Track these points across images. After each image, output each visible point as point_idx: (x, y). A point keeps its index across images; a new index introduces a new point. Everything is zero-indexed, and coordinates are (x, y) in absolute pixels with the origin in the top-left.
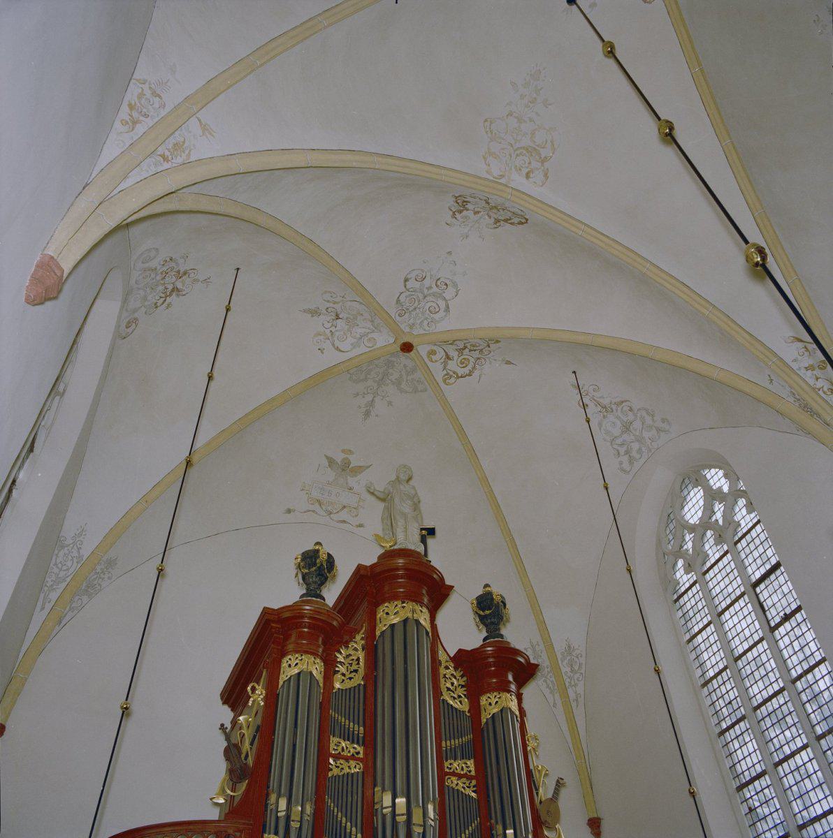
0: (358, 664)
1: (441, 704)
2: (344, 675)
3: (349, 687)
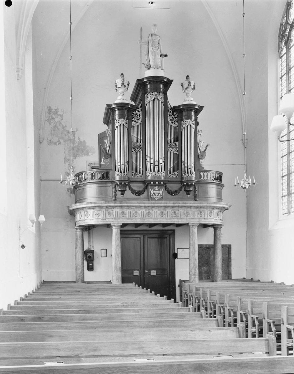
0: (140, 116)
1: (168, 125)
2: (135, 121)
3: (137, 125)
